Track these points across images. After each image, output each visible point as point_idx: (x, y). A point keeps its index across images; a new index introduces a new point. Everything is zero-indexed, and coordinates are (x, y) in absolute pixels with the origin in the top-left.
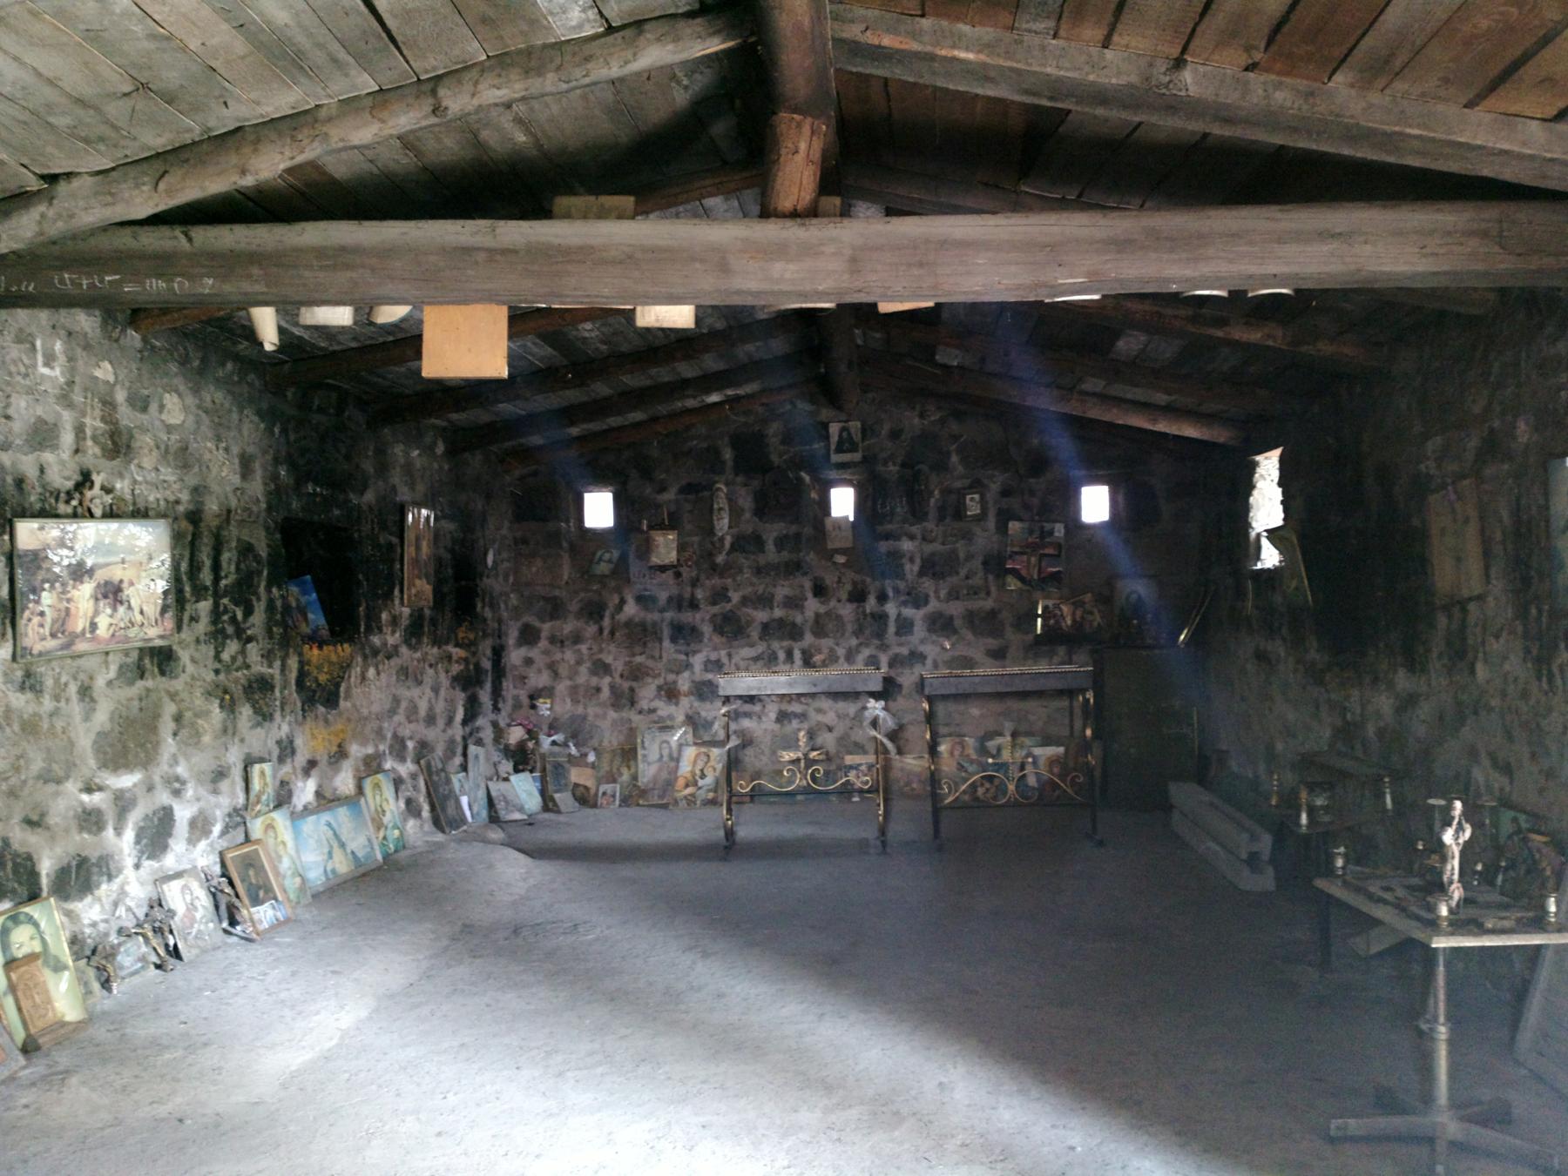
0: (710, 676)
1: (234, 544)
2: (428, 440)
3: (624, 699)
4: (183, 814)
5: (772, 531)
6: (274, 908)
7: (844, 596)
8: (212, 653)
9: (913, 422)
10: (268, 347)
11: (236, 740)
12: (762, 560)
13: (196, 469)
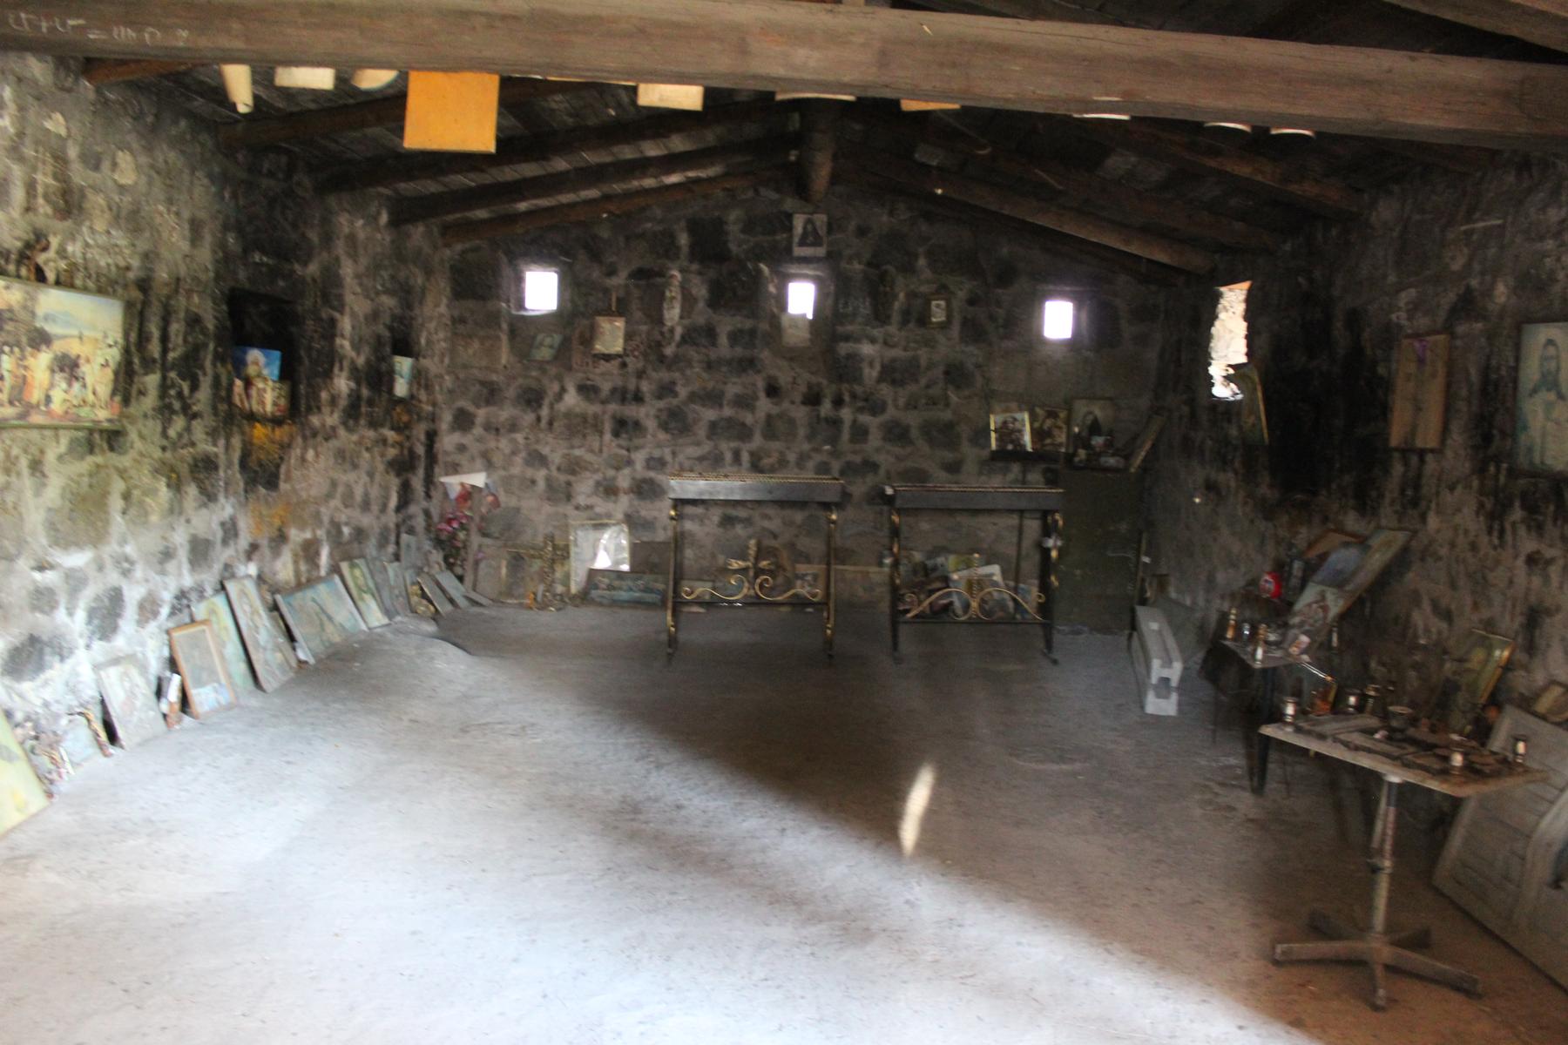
0: (652, 474)
1: (182, 315)
2: (373, 209)
3: (560, 493)
4: (133, 594)
5: (726, 324)
6: (217, 692)
7: (798, 398)
8: (159, 429)
9: (882, 220)
10: (242, 109)
12: (713, 354)
13: (147, 234)
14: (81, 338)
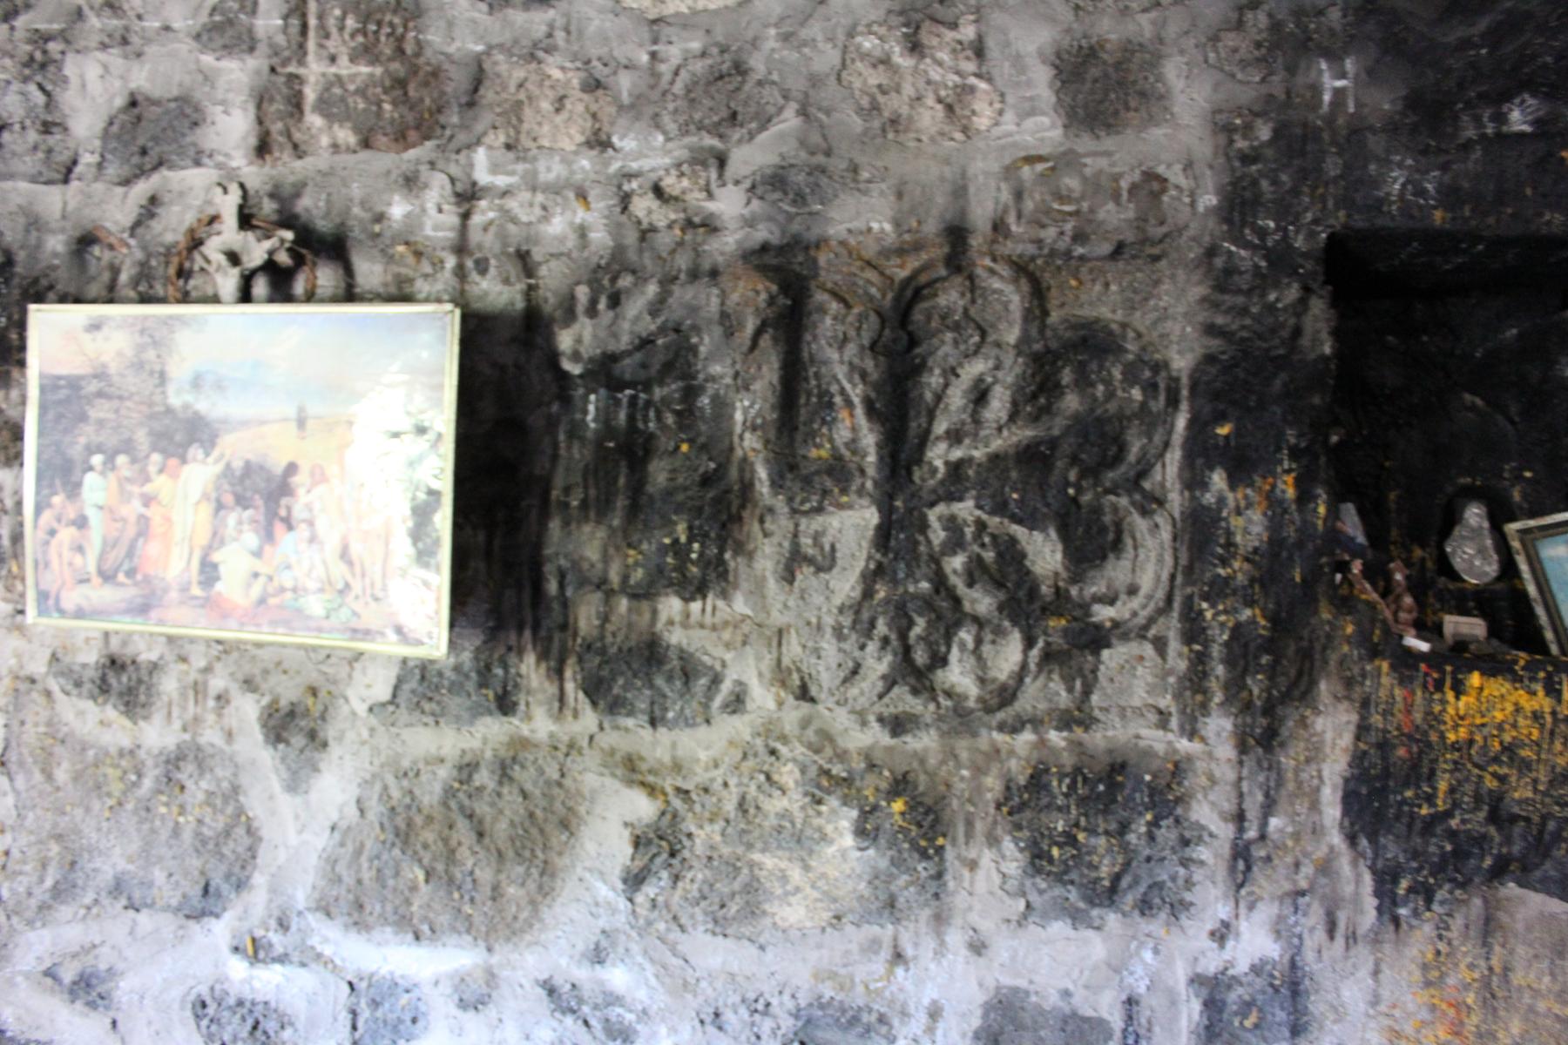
11: (956, 938)
14: (301, 423)
